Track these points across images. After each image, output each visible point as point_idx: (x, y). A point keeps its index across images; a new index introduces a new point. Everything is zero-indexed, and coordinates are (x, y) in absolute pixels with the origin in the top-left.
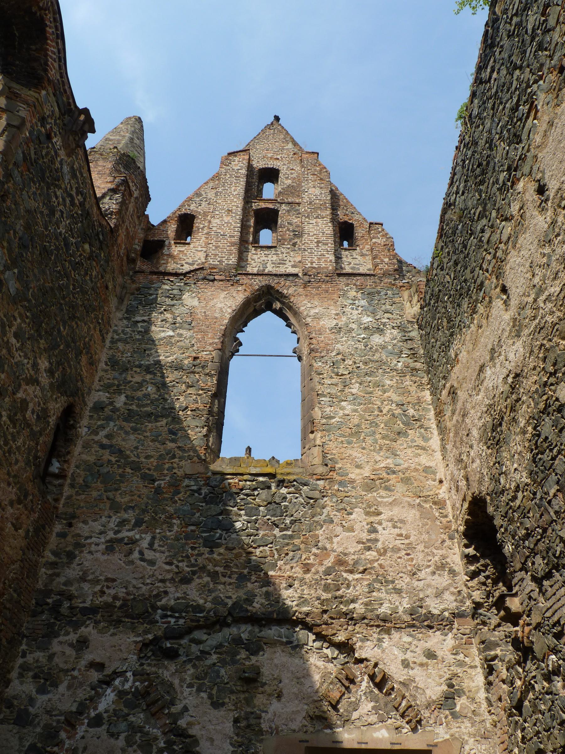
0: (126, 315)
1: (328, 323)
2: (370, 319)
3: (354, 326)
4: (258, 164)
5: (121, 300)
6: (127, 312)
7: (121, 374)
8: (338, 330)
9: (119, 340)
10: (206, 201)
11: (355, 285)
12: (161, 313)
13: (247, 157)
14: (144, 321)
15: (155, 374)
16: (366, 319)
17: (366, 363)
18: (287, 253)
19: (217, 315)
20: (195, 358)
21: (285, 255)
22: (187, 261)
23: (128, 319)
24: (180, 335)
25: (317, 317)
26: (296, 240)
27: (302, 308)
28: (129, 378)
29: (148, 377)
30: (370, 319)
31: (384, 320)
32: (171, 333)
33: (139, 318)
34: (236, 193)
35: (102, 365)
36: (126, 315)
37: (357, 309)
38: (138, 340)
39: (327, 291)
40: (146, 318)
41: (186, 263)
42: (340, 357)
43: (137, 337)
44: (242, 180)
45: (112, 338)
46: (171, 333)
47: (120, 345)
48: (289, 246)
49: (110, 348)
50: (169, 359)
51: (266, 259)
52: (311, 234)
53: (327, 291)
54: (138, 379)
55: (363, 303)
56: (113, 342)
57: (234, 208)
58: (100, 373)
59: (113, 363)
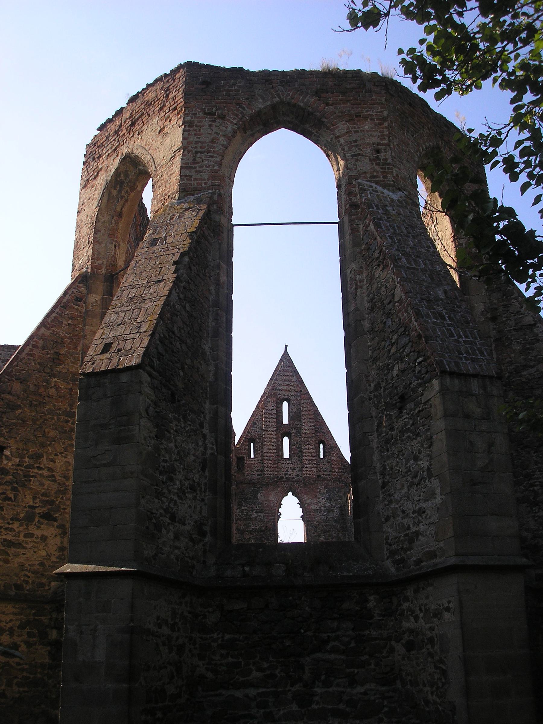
0: (238, 507)
1: (313, 507)
2: (329, 505)
3: (323, 508)
4: (281, 395)
5: (235, 500)
6: (239, 505)
7: (242, 535)
8: (316, 510)
9: (238, 519)
10: (258, 428)
11: (324, 486)
12: (251, 505)
13: (275, 399)
14: (245, 509)
15: (253, 534)
16: (328, 505)
17: (326, 526)
18: (297, 462)
19: (272, 504)
20: (266, 527)
21: (295, 463)
22: (255, 469)
23: (240, 508)
24: (260, 516)
25: (309, 504)
26: (300, 454)
27: (304, 500)
28: (245, 537)
29: (252, 536)
30: (329, 505)
31: (334, 505)
32: (256, 515)
33: (243, 508)
34: (272, 428)
35: (235, 532)
36: (238, 507)
37: (324, 499)
38: (245, 519)
39: (313, 490)
40: (245, 508)
41: (255, 470)
42: (317, 524)
43: (244, 517)
44: (274, 417)
45: (235, 518)
46: (256, 515)
47: (239, 522)
48: (297, 458)
49: (236, 524)
50: (258, 527)
51: (288, 466)
52: (306, 455)
53: (313, 490)
54: (248, 537)
55: (327, 496)
56: (236, 520)
57: (273, 439)
58: (235, 535)
59: (238, 529)
